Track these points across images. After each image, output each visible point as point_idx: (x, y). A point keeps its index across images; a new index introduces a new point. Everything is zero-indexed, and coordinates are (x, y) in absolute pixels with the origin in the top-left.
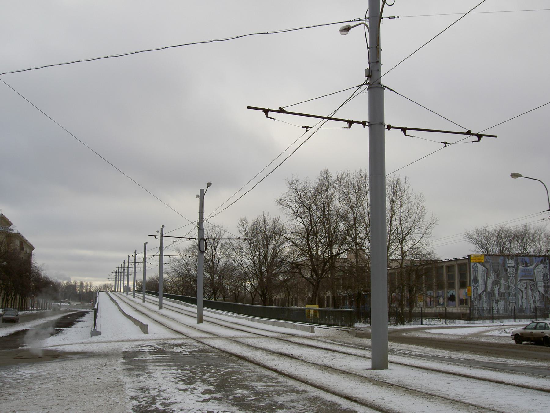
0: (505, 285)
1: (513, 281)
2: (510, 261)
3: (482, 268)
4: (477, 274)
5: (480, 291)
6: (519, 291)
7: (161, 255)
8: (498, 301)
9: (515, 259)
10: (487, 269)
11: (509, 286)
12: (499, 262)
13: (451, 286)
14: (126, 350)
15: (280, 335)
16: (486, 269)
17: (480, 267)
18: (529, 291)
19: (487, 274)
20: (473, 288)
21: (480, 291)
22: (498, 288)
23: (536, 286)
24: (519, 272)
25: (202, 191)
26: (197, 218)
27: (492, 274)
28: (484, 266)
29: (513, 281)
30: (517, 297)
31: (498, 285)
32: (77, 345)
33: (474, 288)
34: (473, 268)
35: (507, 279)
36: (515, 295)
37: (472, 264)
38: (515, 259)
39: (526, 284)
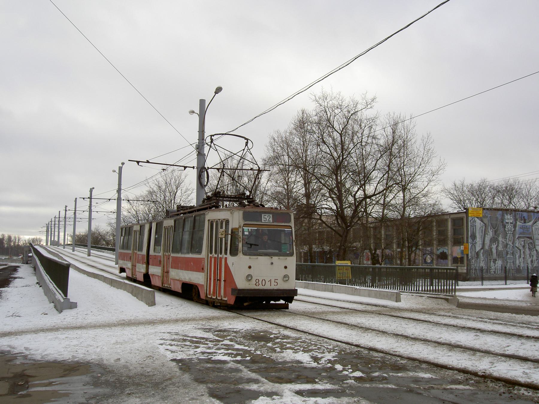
0: (503, 242)
1: (512, 238)
2: (509, 217)
3: (480, 223)
4: (474, 230)
5: (478, 249)
6: (517, 249)
7: (119, 200)
8: (496, 260)
9: (513, 214)
10: (485, 224)
11: (507, 244)
12: (497, 217)
13: (443, 242)
14: (170, 356)
15: (374, 308)
16: (484, 225)
17: (478, 222)
18: (527, 250)
19: (485, 229)
20: (470, 246)
21: (478, 249)
22: (496, 245)
23: (533, 244)
24: (517, 228)
25: (202, 102)
26: (195, 139)
27: (490, 230)
28: (482, 221)
29: (512, 238)
30: (514, 256)
31: (496, 243)
32: (50, 335)
33: (472, 246)
34: (471, 223)
35: (505, 237)
36: (513, 254)
37: (470, 219)
38: (513, 214)
39: (524, 243)
